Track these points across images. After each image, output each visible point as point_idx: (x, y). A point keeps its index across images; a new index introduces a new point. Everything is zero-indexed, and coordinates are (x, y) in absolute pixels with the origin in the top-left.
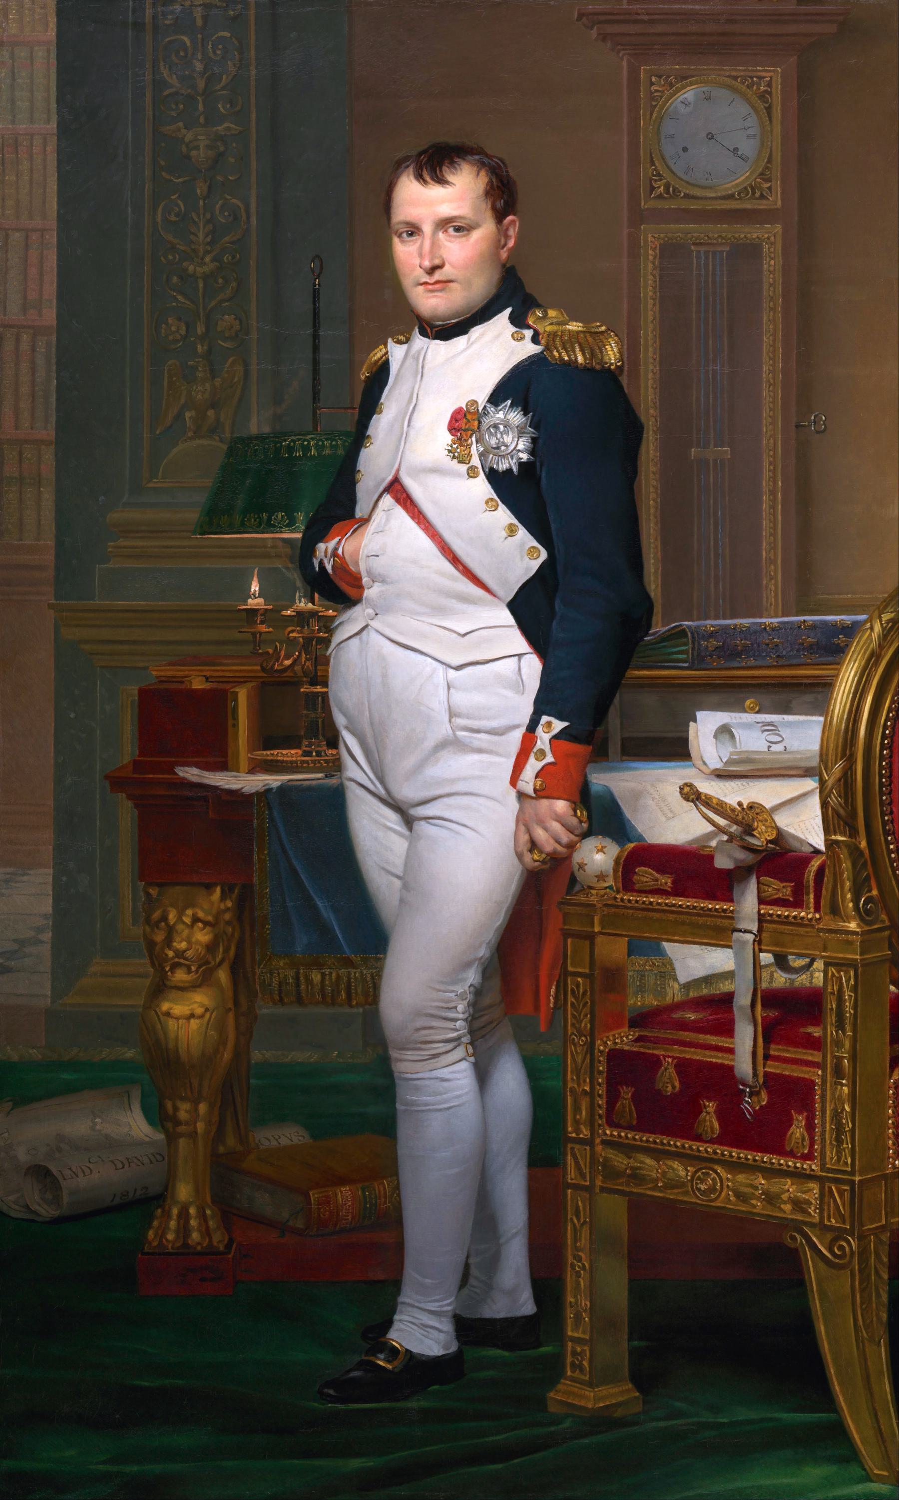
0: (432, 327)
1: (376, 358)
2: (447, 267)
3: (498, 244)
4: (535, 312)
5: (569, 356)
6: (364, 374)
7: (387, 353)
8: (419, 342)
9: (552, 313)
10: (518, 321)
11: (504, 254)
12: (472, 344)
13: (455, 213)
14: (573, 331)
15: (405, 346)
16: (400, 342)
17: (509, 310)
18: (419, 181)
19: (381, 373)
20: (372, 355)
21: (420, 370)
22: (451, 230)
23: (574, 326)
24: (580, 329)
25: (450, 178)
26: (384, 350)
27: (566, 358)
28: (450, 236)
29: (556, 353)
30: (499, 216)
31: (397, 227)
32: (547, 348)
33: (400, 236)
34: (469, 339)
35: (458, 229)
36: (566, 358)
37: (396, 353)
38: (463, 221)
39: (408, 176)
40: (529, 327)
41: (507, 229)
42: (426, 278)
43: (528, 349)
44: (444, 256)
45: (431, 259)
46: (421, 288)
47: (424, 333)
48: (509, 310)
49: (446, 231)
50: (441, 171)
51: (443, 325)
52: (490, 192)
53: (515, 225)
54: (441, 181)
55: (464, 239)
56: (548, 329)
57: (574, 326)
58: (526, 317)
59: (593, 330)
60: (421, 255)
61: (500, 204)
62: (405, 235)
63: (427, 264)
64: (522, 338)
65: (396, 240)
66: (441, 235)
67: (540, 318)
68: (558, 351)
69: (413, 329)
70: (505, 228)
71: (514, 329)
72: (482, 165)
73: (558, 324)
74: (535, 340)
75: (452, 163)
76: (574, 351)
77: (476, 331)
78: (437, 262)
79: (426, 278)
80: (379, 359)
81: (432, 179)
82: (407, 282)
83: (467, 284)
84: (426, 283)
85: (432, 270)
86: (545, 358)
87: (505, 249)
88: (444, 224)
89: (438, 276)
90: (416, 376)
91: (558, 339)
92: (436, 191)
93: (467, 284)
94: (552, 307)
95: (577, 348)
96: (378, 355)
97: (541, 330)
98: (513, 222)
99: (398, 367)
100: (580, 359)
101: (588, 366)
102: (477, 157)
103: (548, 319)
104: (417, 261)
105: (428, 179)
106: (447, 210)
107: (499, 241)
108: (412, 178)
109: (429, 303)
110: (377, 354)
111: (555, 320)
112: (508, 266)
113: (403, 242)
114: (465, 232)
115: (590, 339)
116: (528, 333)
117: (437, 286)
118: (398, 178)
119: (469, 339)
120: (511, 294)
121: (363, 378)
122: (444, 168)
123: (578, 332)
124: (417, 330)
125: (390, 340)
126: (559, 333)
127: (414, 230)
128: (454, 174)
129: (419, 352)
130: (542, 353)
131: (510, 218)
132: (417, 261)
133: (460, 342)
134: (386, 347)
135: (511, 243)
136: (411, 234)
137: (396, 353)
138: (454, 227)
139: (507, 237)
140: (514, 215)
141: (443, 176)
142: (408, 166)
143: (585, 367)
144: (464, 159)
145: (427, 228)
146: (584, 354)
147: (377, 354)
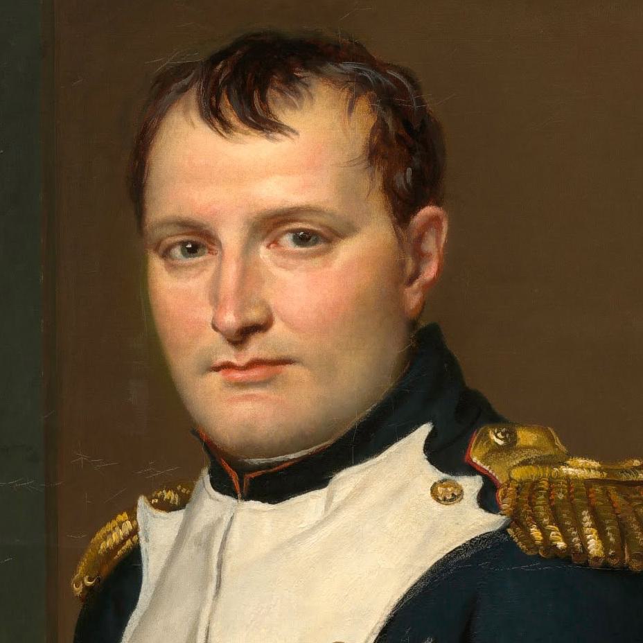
0: (242, 470)
1: (108, 543)
2: (278, 328)
3: (399, 274)
4: (485, 436)
5: (567, 538)
6: (81, 581)
7: (135, 531)
8: (212, 505)
9: (526, 437)
10: (447, 455)
11: (413, 298)
12: (338, 509)
13: (297, 199)
14: (576, 480)
15: (178, 516)
16: (167, 507)
17: (425, 430)
18: (212, 125)
19: (122, 580)
20: (99, 535)
21: (215, 573)
22: (287, 240)
23: (580, 469)
24: (594, 475)
25: (286, 117)
26: (128, 526)
27: (561, 544)
28: (285, 254)
29: (535, 533)
30: (402, 207)
31: (158, 233)
32: (516, 520)
33: (166, 254)
34: (330, 499)
35: (303, 238)
36: (561, 544)
37: (158, 530)
38: (317, 218)
39: (186, 112)
40: (472, 470)
41: (420, 239)
42: (228, 355)
43: (470, 521)
44: (272, 302)
45: (240, 311)
46: (216, 378)
47: (222, 485)
48: (425, 430)
49: (275, 242)
50: (263, 100)
51: (269, 466)
52: (378, 151)
53: (439, 229)
54: (265, 124)
55: (318, 261)
56: (518, 474)
57: (580, 469)
58: (466, 447)
59: (624, 478)
60: (216, 300)
61: (403, 178)
62: (177, 252)
63: (230, 319)
64: (456, 497)
65: (157, 264)
66: (264, 252)
67: (497, 449)
68: (541, 528)
69: (196, 476)
70: (415, 235)
71: (437, 475)
72: (359, 85)
73: (542, 462)
74: (487, 500)
75: (290, 83)
76: (579, 526)
77: (347, 480)
78: (254, 315)
79: (228, 355)
80: (117, 547)
81: (243, 119)
82: (184, 364)
83: (326, 368)
84: (228, 366)
85: (242, 336)
86: (511, 543)
87: (416, 285)
88: (268, 224)
89: (256, 348)
90: (204, 587)
91: (541, 499)
92: (250, 148)
93: (326, 368)
94: (528, 424)
95: (587, 520)
96: (115, 538)
97: (501, 478)
98: (434, 221)
99: (162, 563)
100: (594, 546)
101: (614, 562)
102: (349, 67)
103: (517, 451)
104: (207, 314)
105: (233, 118)
106: (277, 192)
107: (402, 265)
108: (195, 116)
109: (237, 413)
110: (113, 535)
111: (533, 454)
112: (423, 324)
113: (172, 267)
114: (321, 246)
115: (617, 499)
116: (471, 485)
117: (255, 373)
118: (162, 116)
119: (330, 499)
120: (433, 390)
121: (78, 590)
122: (272, 94)
123: (589, 483)
124: (206, 477)
125: (142, 501)
126: (545, 484)
127: (198, 240)
128: (293, 107)
129: (211, 529)
130: (503, 531)
131: (428, 211)
132: (207, 314)
133: (310, 504)
134: (133, 517)
135: (430, 271)
136: (193, 250)
137: (158, 530)
138: (295, 232)
139: (421, 257)
140: (438, 204)
141: (268, 111)
142: (185, 89)
143: (606, 565)
144: (318, 73)
145: (231, 236)
146: (602, 535)
147: (113, 535)
